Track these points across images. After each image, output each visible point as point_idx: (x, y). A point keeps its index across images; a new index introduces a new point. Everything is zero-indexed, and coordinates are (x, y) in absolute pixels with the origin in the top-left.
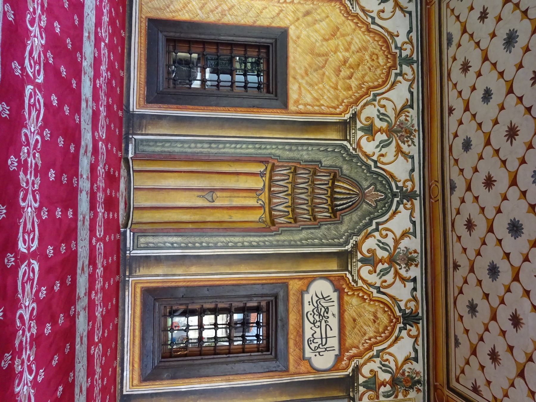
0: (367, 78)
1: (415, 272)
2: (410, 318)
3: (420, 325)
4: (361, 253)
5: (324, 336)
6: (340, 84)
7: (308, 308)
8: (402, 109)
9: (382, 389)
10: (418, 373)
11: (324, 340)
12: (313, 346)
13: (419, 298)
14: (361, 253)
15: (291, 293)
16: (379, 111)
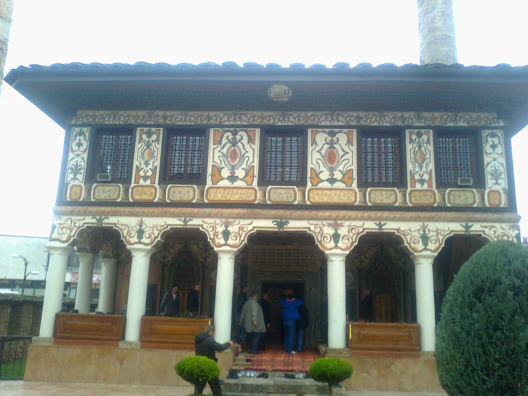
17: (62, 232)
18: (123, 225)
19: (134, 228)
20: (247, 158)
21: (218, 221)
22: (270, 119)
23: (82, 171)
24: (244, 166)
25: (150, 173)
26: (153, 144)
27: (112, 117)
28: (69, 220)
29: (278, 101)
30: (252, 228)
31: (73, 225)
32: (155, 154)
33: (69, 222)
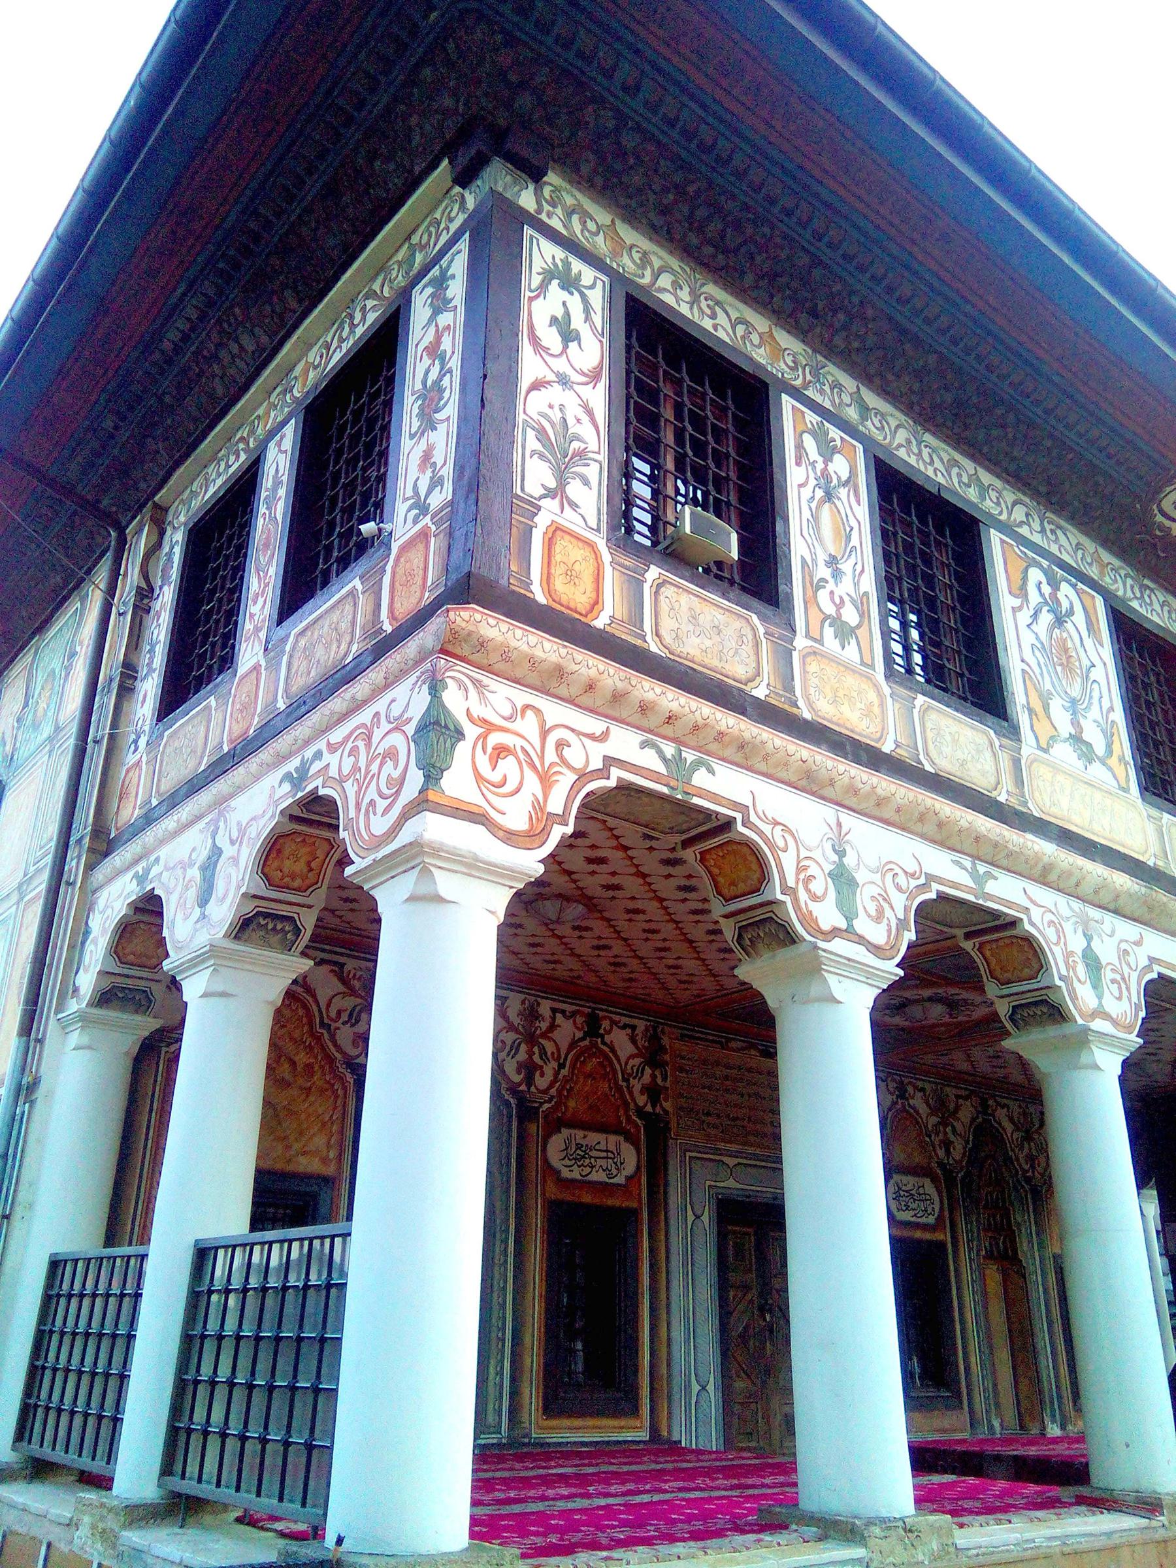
0: (297, 1034)
1: (545, 1008)
2: (593, 1027)
3: (601, 1014)
4: (520, 1084)
5: (604, 1154)
6: (300, 1081)
7: (576, 1174)
8: (344, 981)
9: (659, 1081)
10: (647, 1029)
11: (610, 1155)
12: (614, 1172)
13: (574, 1008)
14: (520, 1084)
15: (560, 1196)
16: (345, 1023)
17: (496, 777)
18: (777, 823)
19: (817, 854)
20: (1095, 686)
21: (1062, 903)
22: (1115, 581)
23: (592, 472)
24: (1095, 713)
25: (850, 616)
26: (843, 492)
27: (686, 289)
28: (529, 713)
29: (1161, 527)
30: (1146, 962)
31: (551, 756)
32: (855, 541)
33: (528, 726)
